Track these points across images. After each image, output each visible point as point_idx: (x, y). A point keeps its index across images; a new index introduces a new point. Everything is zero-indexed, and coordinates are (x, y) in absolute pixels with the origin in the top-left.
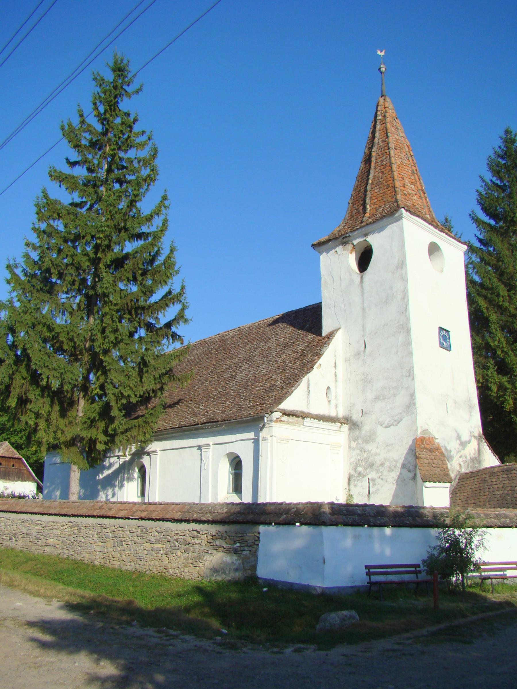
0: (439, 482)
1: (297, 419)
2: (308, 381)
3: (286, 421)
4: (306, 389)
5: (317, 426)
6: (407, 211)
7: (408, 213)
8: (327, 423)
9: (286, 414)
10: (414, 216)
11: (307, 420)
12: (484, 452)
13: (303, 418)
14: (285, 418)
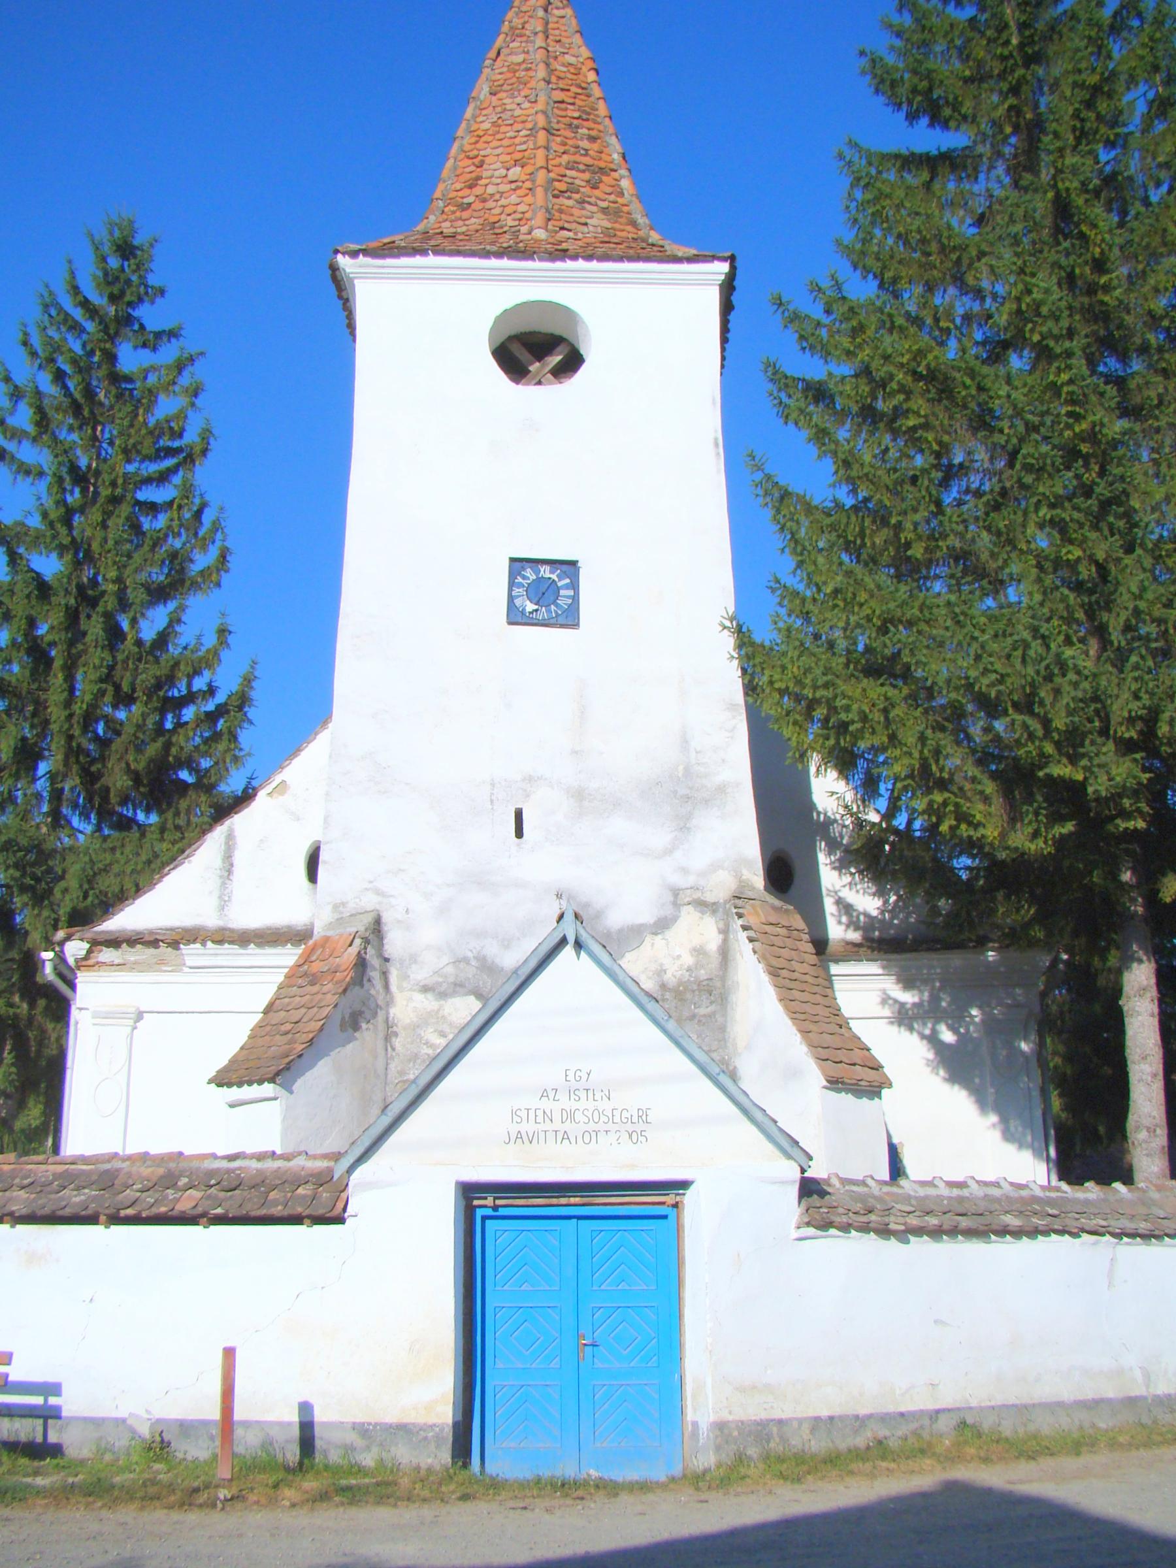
0: (250, 1083)
1: (152, 951)
2: (230, 837)
3: (116, 962)
4: (218, 862)
5: (220, 961)
6: (354, 254)
8: (279, 950)
9: (114, 942)
10: (397, 256)
11: (192, 953)
12: (738, 956)
13: (175, 944)
14: (107, 955)
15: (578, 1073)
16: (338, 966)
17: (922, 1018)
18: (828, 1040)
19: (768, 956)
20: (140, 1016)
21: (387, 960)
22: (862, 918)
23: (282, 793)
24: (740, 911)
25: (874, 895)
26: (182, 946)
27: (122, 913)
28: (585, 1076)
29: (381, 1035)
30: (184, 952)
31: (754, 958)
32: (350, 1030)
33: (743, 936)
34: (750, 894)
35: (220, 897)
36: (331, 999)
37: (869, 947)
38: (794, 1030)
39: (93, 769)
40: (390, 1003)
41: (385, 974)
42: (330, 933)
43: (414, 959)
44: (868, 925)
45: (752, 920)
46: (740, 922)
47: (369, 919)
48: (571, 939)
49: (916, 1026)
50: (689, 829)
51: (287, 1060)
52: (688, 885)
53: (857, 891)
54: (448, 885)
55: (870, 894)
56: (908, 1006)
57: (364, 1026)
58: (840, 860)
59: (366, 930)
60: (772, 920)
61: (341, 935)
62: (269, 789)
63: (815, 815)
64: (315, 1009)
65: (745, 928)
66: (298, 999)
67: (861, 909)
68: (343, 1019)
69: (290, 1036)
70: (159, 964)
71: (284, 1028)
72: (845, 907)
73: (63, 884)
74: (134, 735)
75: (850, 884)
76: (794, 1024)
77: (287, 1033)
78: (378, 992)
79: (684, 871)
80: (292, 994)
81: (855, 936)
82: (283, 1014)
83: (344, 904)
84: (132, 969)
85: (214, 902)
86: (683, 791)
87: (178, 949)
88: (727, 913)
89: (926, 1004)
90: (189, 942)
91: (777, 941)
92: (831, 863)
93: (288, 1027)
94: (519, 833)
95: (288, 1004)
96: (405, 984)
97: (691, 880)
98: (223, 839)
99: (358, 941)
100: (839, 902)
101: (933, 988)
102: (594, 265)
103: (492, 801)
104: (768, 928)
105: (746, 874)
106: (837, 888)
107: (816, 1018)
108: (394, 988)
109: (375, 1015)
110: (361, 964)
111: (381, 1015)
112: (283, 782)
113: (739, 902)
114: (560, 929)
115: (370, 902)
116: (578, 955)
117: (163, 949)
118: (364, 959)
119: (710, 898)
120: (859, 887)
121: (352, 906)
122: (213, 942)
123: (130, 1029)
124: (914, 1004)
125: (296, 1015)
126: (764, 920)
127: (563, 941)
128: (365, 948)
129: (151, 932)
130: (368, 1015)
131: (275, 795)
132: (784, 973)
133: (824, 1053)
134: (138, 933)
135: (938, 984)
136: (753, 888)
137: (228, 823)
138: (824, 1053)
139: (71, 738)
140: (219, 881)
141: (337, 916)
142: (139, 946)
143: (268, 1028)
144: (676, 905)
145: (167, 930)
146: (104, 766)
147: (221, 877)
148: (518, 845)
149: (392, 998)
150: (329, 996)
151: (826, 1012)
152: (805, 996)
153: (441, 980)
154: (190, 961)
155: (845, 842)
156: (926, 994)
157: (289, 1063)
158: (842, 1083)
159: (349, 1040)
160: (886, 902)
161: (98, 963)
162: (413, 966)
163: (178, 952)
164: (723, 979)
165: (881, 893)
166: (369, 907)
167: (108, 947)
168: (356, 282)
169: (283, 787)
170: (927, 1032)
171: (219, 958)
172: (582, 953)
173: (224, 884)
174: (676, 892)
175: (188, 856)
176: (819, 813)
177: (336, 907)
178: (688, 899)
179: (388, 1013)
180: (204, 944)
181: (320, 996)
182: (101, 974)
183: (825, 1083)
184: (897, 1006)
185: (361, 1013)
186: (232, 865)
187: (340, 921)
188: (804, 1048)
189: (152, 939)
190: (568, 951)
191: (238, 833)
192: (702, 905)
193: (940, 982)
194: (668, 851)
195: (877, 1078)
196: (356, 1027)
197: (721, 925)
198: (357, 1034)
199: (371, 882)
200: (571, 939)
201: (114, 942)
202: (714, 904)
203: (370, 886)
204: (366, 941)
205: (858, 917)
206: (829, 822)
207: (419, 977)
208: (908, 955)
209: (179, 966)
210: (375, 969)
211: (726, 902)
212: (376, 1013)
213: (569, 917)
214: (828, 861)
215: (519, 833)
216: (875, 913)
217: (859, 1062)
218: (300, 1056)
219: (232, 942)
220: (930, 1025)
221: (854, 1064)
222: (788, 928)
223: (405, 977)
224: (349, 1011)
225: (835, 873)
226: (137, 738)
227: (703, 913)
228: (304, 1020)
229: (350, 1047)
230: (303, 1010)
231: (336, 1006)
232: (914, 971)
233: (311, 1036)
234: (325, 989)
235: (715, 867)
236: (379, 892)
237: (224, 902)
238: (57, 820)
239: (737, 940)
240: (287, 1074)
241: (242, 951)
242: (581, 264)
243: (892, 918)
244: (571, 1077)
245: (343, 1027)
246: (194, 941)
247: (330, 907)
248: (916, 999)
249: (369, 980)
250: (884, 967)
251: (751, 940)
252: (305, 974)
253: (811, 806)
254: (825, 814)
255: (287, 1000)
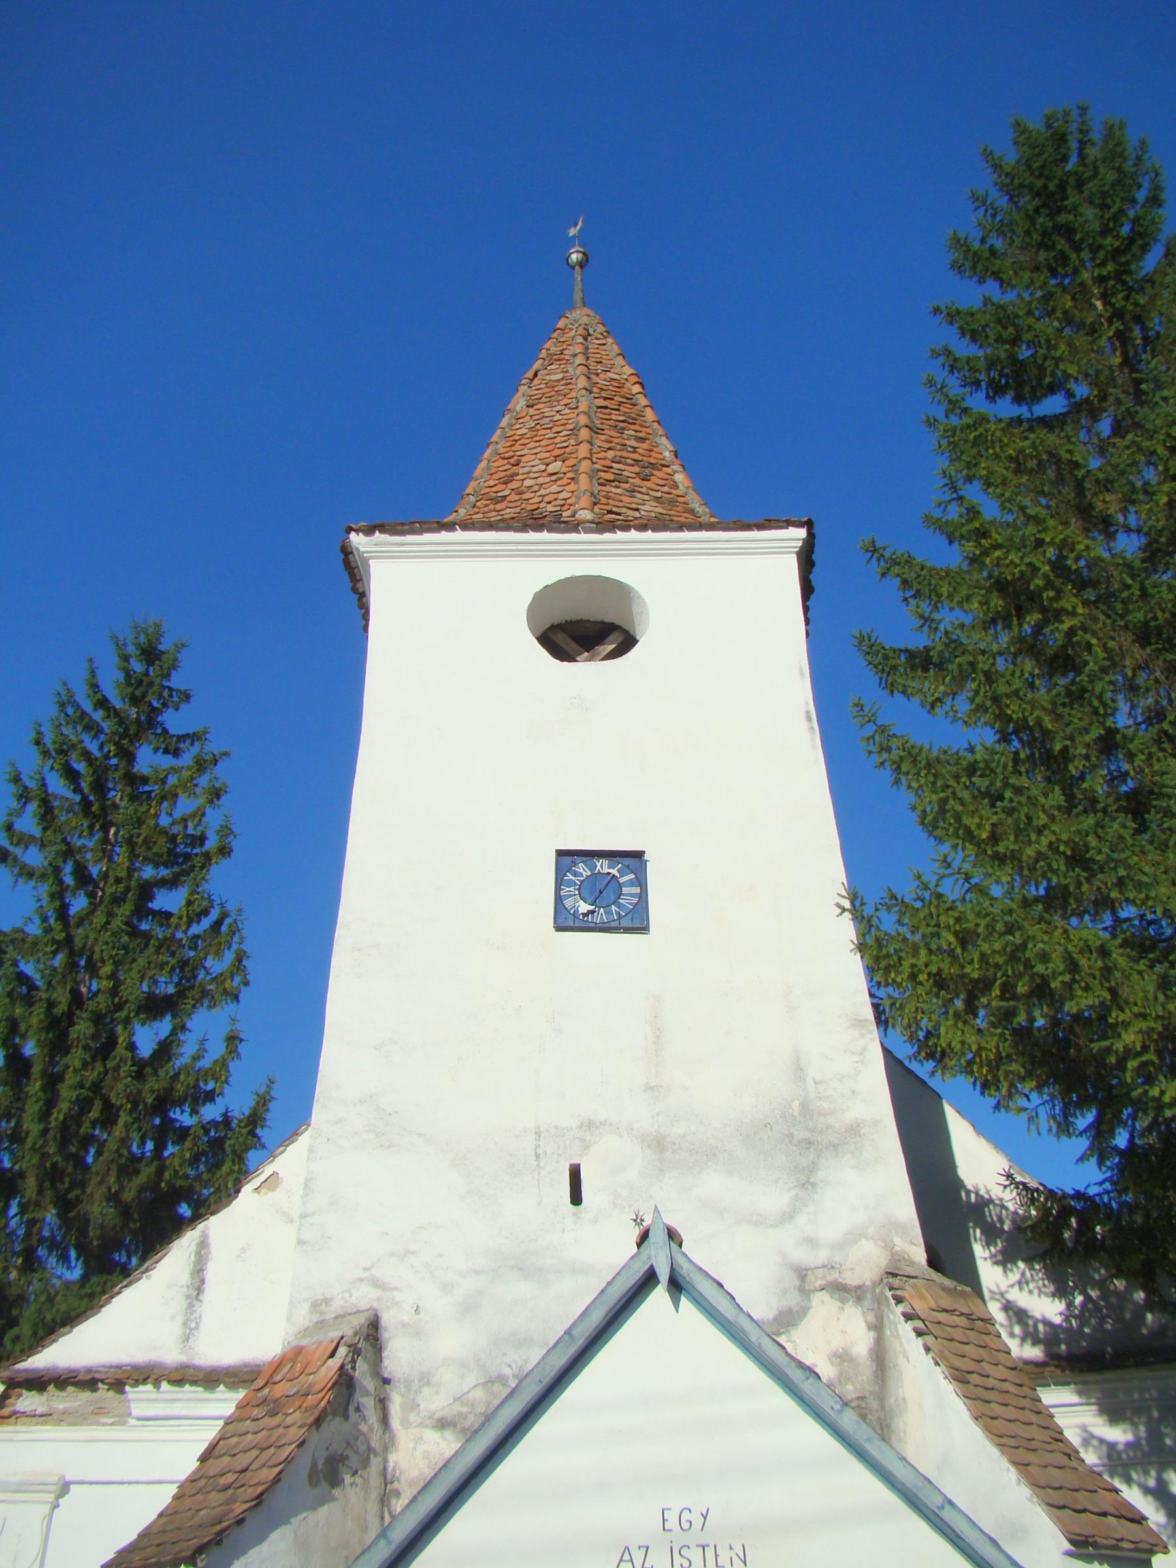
1: (87, 1395)
2: (203, 1245)
3: (40, 1410)
4: (185, 1278)
6: (369, 531)
7: (378, 536)
9: (38, 1382)
10: (420, 532)
11: (140, 1398)
12: (901, 1359)
13: (118, 1385)
14: (28, 1401)
15: (686, 1514)
16: (311, 1385)
17: (1142, 1464)
18: (1057, 1476)
19: (948, 1354)
20: (64, 1488)
21: (387, 1381)
22: (1041, 1327)
23: (273, 1188)
24: (898, 1293)
25: (1053, 1295)
26: (127, 1388)
27: (55, 1345)
28: (698, 1521)
29: (375, 1494)
30: (130, 1396)
31: (928, 1360)
32: (325, 1485)
33: (906, 1329)
34: (909, 1271)
35: (185, 1324)
36: (295, 1434)
37: (1056, 1366)
38: (1004, 1463)
39: (71, 1196)
40: (389, 1444)
41: (383, 1403)
42: (304, 1342)
43: (426, 1379)
44: (1050, 1337)
45: (920, 1307)
46: (900, 1309)
47: (361, 1320)
48: (663, 1274)
49: (1134, 1476)
50: (813, 1185)
51: (218, 1528)
52: (820, 1263)
53: (1031, 1292)
54: (477, 1272)
55: (1046, 1294)
56: (1121, 1447)
57: (348, 1479)
58: (1003, 1252)
59: (355, 1334)
60: (947, 1303)
61: (320, 1343)
62: (256, 1182)
63: (963, 1194)
64: (272, 1450)
65: (908, 1317)
66: (250, 1437)
67: (1038, 1315)
68: (314, 1466)
69: (231, 1491)
70: (96, 1415)
71: (223, 1481)
72: (1019, 1315)
73: (14, 1331)
74: (117, 1151)
75: (1020, 1282)
76: (1003, 1453)
77: (226, 1488)
78: (371, 1429)
79: (811, 1242)
80: (243, 1430)
81: (1034, 1352)
82: (226, 1460)
83: (327, 1301)
84: (60, 1422)
85: (176, 1329)
86: (800, 1134)
87: (122, 1392)
88: (879, 1301)
89: (1144, 1442)
90: (137, 1383)
91: (957, 1334)
92: (992, 1256)
93: (230, 1478)
94: (576, 1197)
95: (236, 1445)
96: (412, 1417)
97: (822, 1256)
98: (193, 1248)
99: (342, 1351)
100: (1008, 1307)
101: (1150, 1419)
102: (649, 535)
103: (537, 1156)
104: (942, 1317)
105: (900, 1244)
106: (1003, 1288)
107: (1034, 1444)
108: (395, 1422)
109: (366, 1463)
110: (345, 1382)
111: (375, 1462)
112: (275, 1174)
113: (896, 1282)
114: (643, 1257)
115: (364, 1298)
116: (676, 1304)
117: (104, 1394)
118: (351, 1378)
119: (851, 1279)
120: (1031, 1286)
121: (337, 1306)
122: (170, 1382)
123: (47, 1507)
124: (1128, 1445)
125: (243, 1460)
126: (933, 1305)
127: (649, 1279)
128: (354, 1361)
129: (89, 1370)
130: (354, 1461)
131: (263, 1190)
132: (974, 1378)
133: (1059, 1497)
134: (71, 1371)
135: (1155, 1414)
136: (912, 1263)
137: (201, 1226)
138: (1059, 1497)
139: (45, 1156)
140: (185, 1303)
141: (316, 1318)
142: (70, 1389)
143: (203, 1481)
144: (804, 1291)
145: (111, 1367)
146: (84, 1192)
147: (188, 1297)
148: (574, 1214)
149: (393, 1439)
150: (293, 1430)
151: (1045, 1436)
152: (1010, 1412)
153: (464, 1410)
154: (137, 1409)
155: (1006, 1227)
156: (1142, 1428)
157: (220, 1533)
158: (1095, 1545)
159: (322, 1503)
160: (1070, 1305)
161: (15, 1413)
162: (426, 1391)
163: (122, 1397)
164: (881, 1397)
165: (1061, 1292)
166: (363, 1305)
167: (30, 1389)
168: (371, 562)
169: (273, 1181)
170: (1151, 1482)
171: (177, 1405)
172: (684, 1301)
173: (191, 1306)
174: (802, 1273)
175: (147, 1270)
176: (968, 1192)
177: (315, 1305)
178: (819, 1283)
179: (385, 1460)
180: (157, 1384)
181: (281, 1430)
182: (19, 1428)
183: (1067, 1546)
184: (1104, 1448)
185: (343, 1458)
186: (203, 1281)
187: (321, 1324)
188: (1025, 1491)
189: (88, 1377)
190: (659, 1295)
191: (212, 1239)
192: (840, 1290)
193: (1159, 1411)
194: (788, 1216)
195: (1143, 1537)
196: (334, 1480)
197: (871, 1317)
198: (336, 1492)
199: (366, 1269)
200: (663, 1274)
201: (38, 1382)
202: (859, 1287)
203: (366, 1274)
204: (355, 1351)
205: (1035, 1326)
206: (984, 1203)
207: (433, 1406)
208: (1110, 1375)
209: (122, 1418)
210: (367, 1394)
211: (874, 1284)
212: (368, 1459)
213: (658, 1237)
214: (987, 1254)
215: (576, 1197)
216: (1057, 1320)
217: (1111, 1510)
218: (240, 1522)
219: (194, 1383)
220: (1153, 1473)
221: (1105, 1514)
222: (968, 1316)
223: (413, 1406)
224: (324, 1454)
225: (998, 1270)
226: (121, 1156)
227: (843, 1301)
228: (253, 1467)
229: (324, 1511)
230: (255, 1453)
231: (302, 1444)
232: (1121, 1396)
233: (260, 1489)
234: (289, 1420)
235: (854, 1236)
236: (377, 1284)
237: (189, 1329)
238: (30, 1263)
239: (898, 1337)
240: (217, 1551)
241: (207, 1395)
242: (633, 534)
243: (1081, 1326)
244: (672, 1522)
245: (313, 1478)
246: (145, 1381)
247: (306, 1306)
248: (1129, 1437)
249: (358, 1409)
250: (1080, 1393)
251: (919, 1333)
252: (265, 1400)
253: (958, 1184)
254: (977, 1193)
255: (235, 1440)
